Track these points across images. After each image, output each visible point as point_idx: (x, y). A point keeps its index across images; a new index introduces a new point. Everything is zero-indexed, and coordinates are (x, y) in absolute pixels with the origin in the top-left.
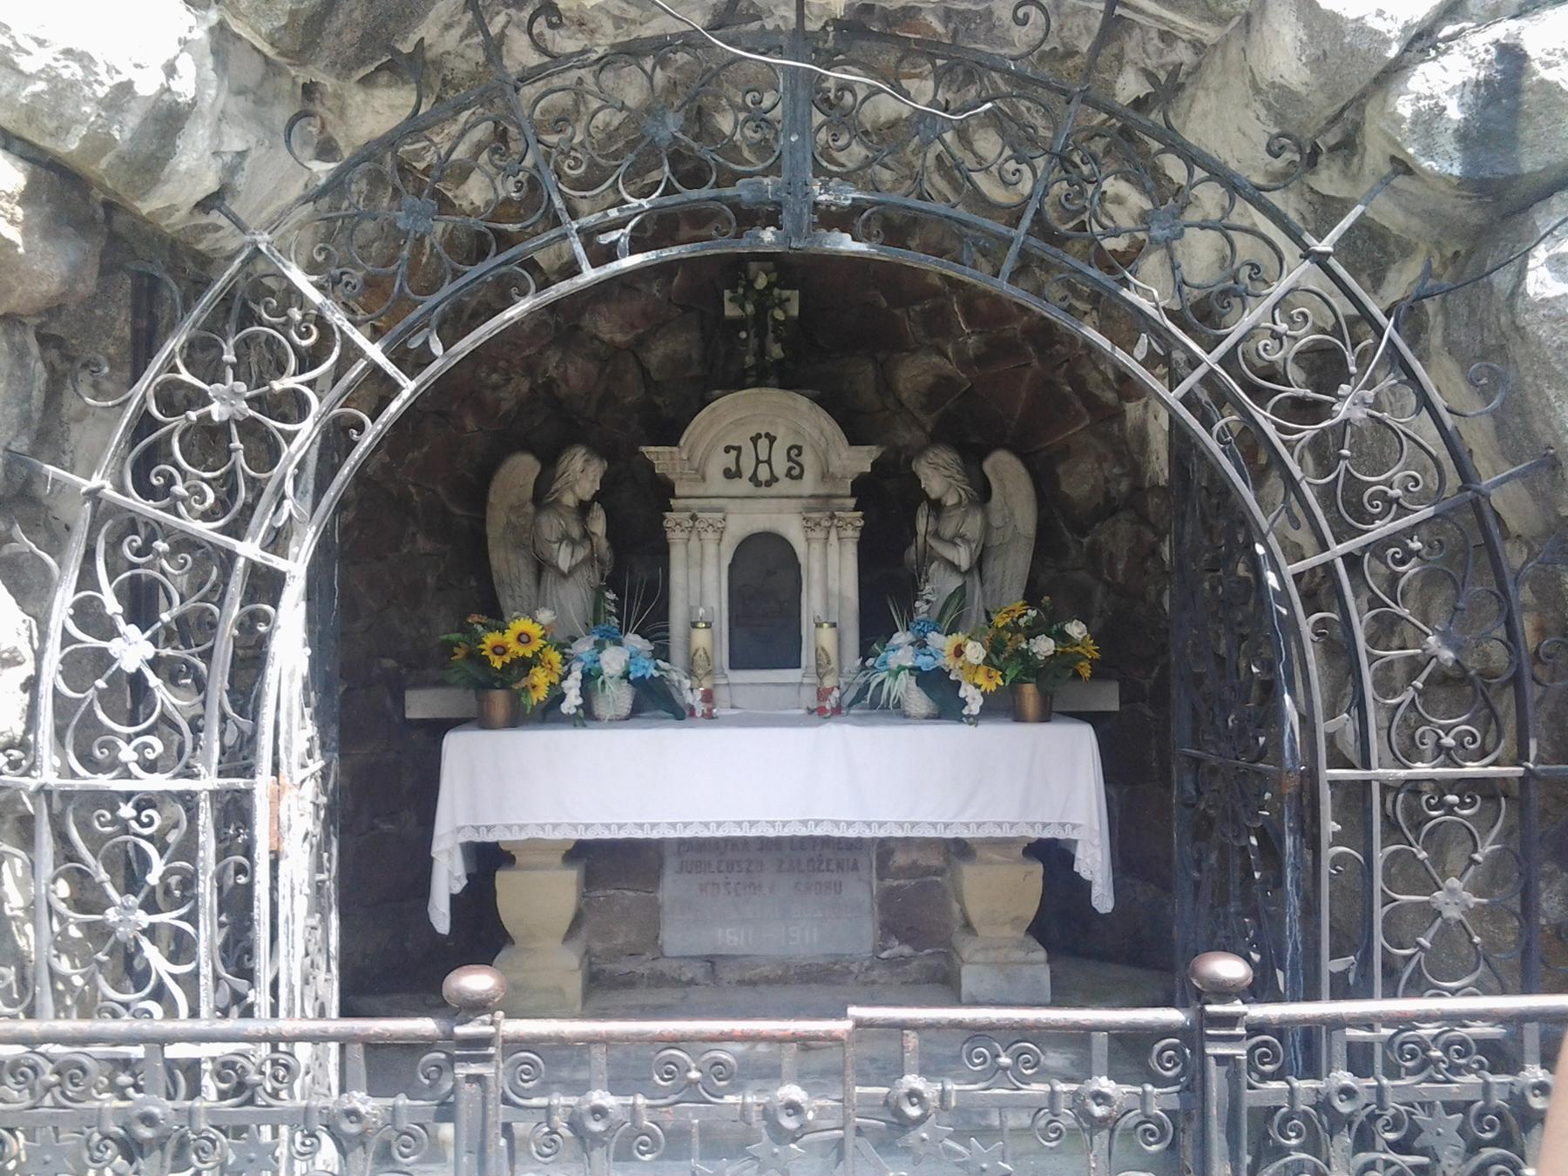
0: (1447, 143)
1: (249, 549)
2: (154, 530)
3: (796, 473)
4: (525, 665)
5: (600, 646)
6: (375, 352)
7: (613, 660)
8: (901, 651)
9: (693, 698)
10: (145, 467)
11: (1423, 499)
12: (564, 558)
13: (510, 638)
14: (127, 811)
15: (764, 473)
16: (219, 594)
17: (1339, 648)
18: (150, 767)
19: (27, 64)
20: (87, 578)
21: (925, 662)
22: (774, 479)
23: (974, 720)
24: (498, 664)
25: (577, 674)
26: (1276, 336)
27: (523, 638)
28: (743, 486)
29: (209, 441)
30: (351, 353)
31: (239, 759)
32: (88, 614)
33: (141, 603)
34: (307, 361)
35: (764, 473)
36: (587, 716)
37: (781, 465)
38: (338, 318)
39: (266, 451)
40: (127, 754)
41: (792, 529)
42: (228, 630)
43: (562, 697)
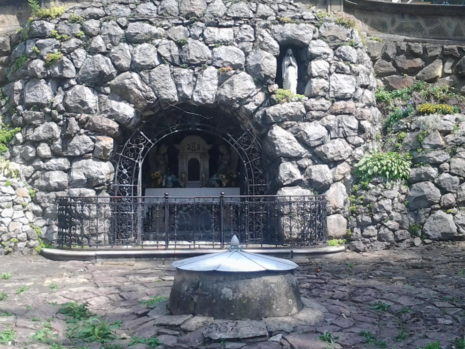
0: (260, 120)
1: (137, 161)
2: (126, 159)
3: (199, 148)
4: (157, 178)
5: (167, 176)
6: (150, 141)
7: (170, 178)
8: (215, 177)
9: (182, 185)
10: (125, 153)
11: (259, 156)
12: (161, 163)
13: (155, 174)
14: (124, 188)
15: (194, 149)
16: (134, 166)
17: (250, 172)
18: (126, 183)
19: (120, 115)
20: (120, 164)
21: (218, 178)
22: (195, 150)
23: (225, 187)
24: (153, 178)
25: (164, 180)
26: (244, 139)
27: (157, 174)
28: (190, 151)
29: (132, 150)
30: (147, 141)
31: (136, 183)
32: (120, 168)
33: (126, 167)
34: (143, 141)
35: (194, 149)
36: (165, 187)
37: (196, 147)
38: (146, 137)
39: (138, 151)
40: (124, 182)
41: (198, 158)
42: (135, 169)
43: (162, 184)
